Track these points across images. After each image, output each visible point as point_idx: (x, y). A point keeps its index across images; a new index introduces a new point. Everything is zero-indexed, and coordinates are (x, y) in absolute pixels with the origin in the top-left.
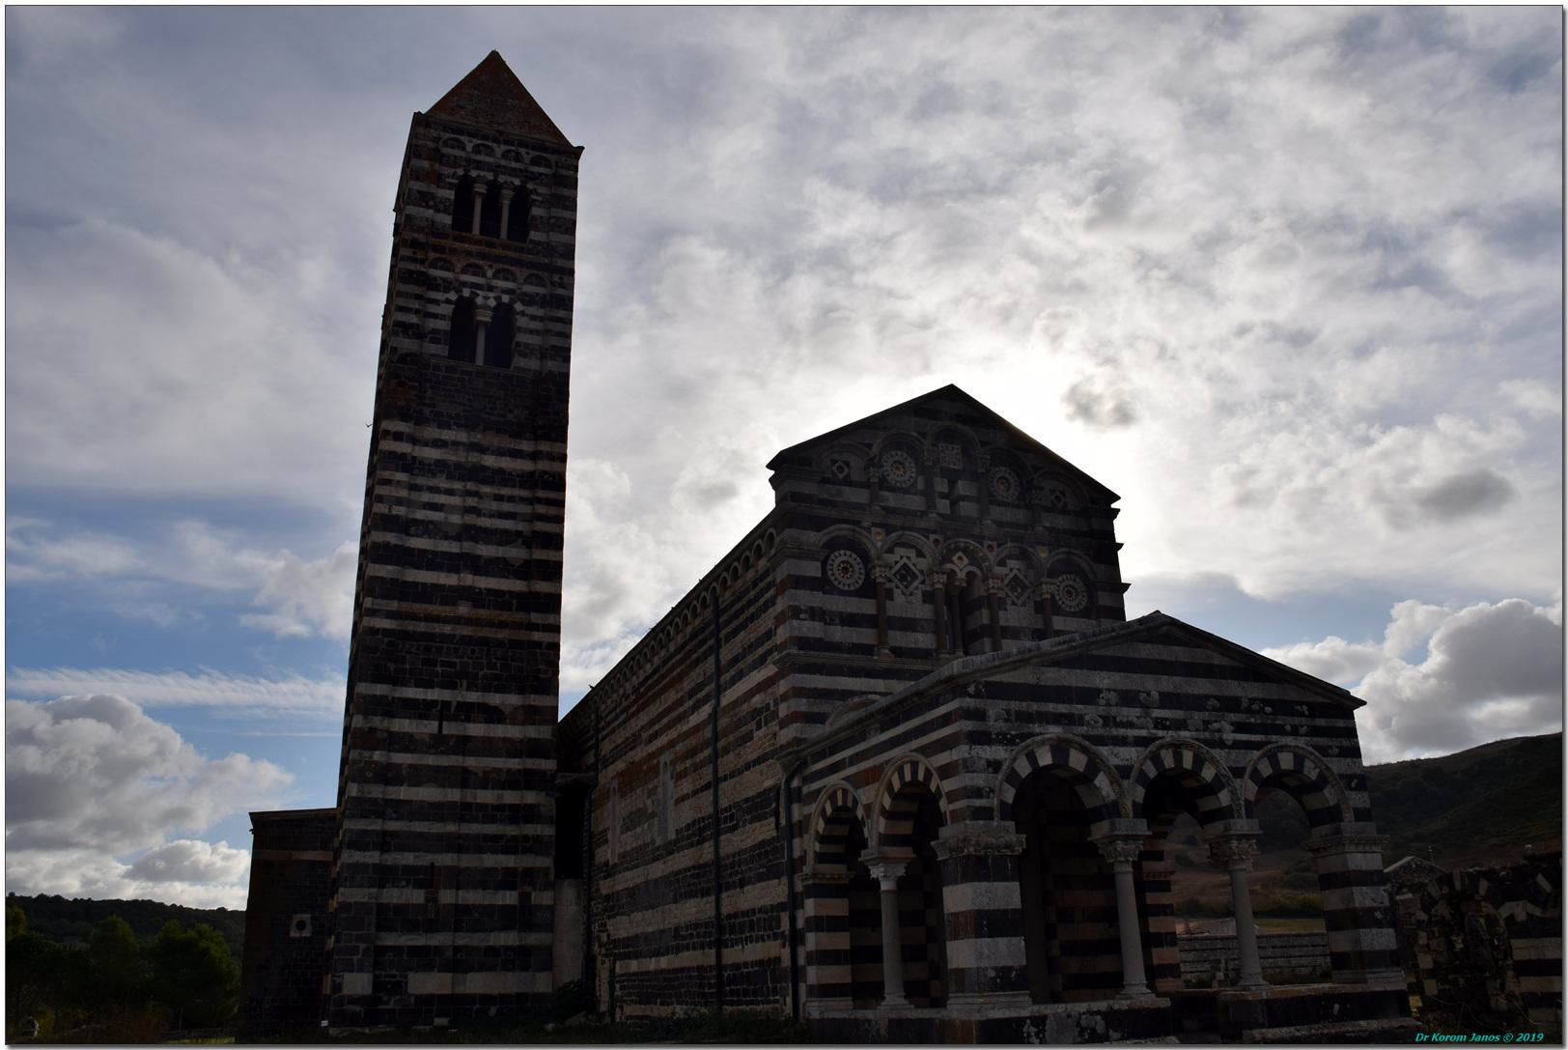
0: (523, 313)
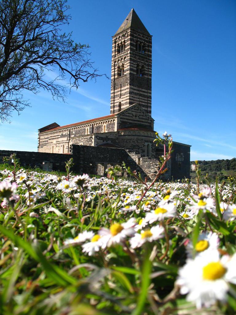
0: (145, 67)
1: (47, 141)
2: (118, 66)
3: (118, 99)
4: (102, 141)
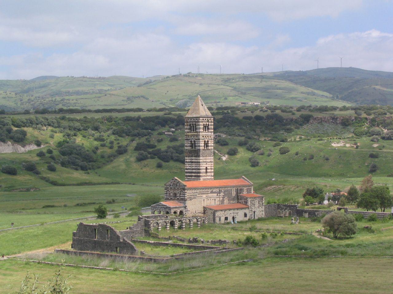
1: (196, 195)
2: (204, 140)
3: (205, 164)
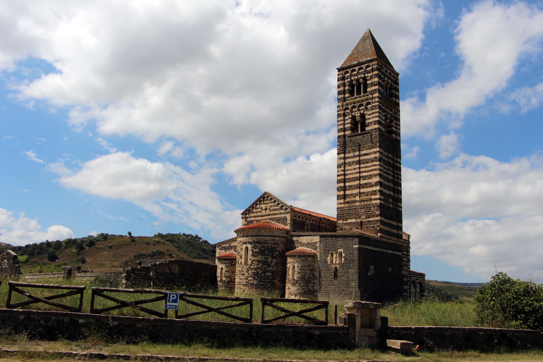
0: (366, 114)
4: (224, 251)
